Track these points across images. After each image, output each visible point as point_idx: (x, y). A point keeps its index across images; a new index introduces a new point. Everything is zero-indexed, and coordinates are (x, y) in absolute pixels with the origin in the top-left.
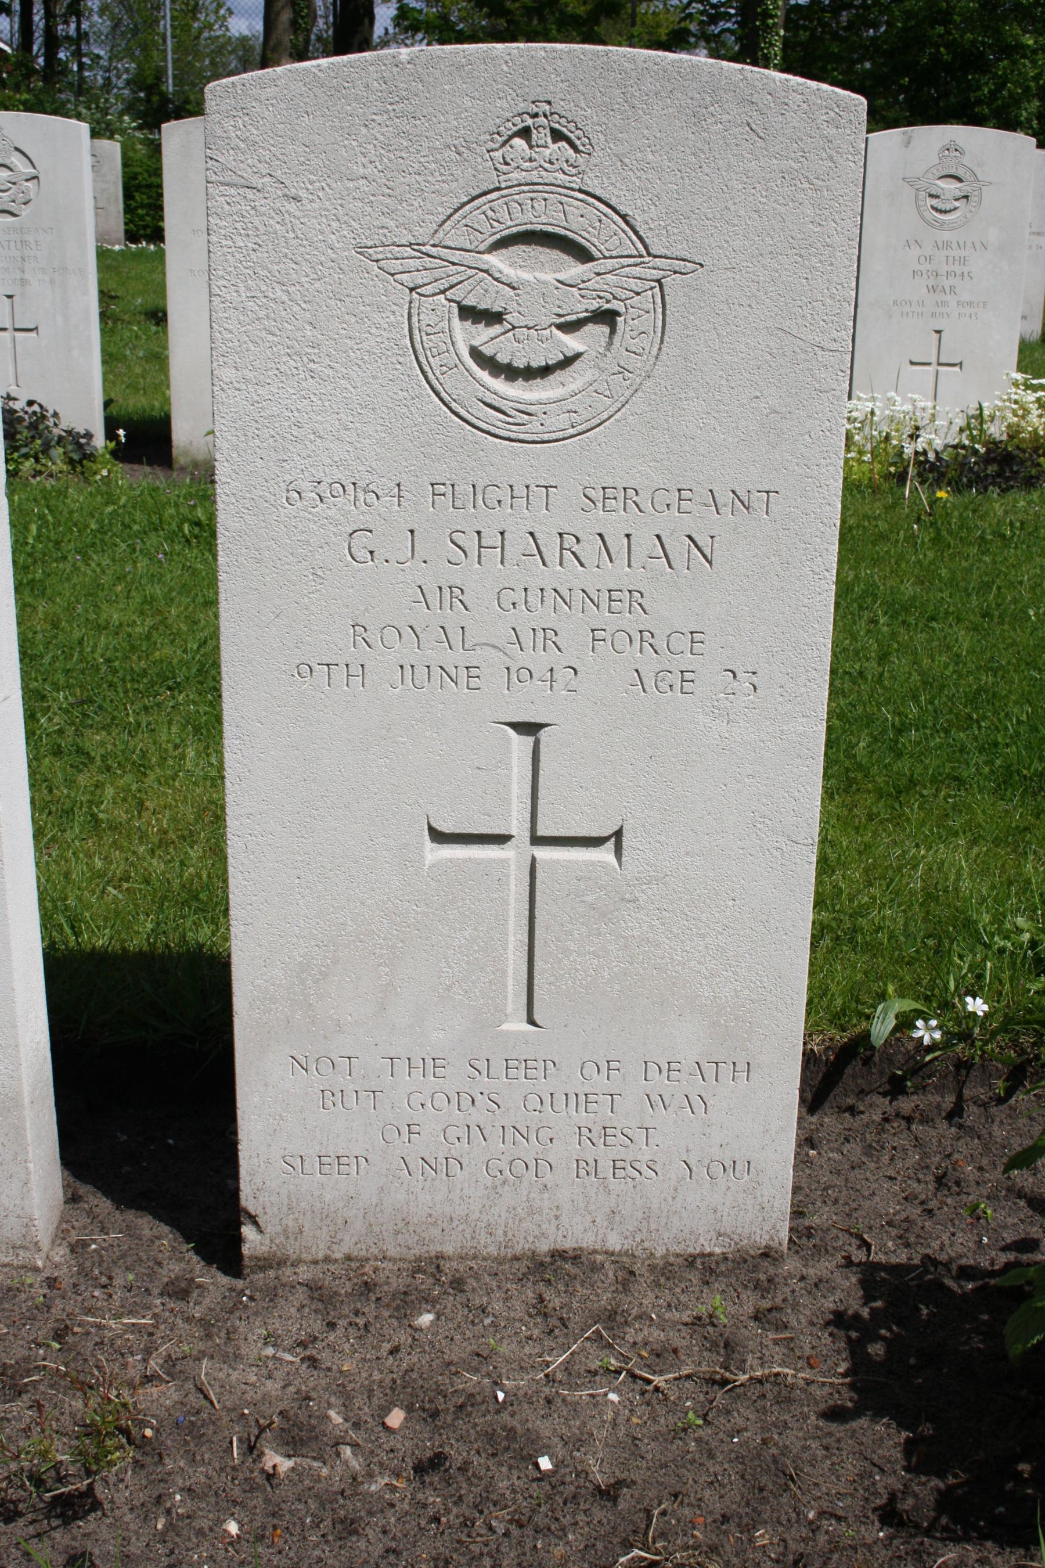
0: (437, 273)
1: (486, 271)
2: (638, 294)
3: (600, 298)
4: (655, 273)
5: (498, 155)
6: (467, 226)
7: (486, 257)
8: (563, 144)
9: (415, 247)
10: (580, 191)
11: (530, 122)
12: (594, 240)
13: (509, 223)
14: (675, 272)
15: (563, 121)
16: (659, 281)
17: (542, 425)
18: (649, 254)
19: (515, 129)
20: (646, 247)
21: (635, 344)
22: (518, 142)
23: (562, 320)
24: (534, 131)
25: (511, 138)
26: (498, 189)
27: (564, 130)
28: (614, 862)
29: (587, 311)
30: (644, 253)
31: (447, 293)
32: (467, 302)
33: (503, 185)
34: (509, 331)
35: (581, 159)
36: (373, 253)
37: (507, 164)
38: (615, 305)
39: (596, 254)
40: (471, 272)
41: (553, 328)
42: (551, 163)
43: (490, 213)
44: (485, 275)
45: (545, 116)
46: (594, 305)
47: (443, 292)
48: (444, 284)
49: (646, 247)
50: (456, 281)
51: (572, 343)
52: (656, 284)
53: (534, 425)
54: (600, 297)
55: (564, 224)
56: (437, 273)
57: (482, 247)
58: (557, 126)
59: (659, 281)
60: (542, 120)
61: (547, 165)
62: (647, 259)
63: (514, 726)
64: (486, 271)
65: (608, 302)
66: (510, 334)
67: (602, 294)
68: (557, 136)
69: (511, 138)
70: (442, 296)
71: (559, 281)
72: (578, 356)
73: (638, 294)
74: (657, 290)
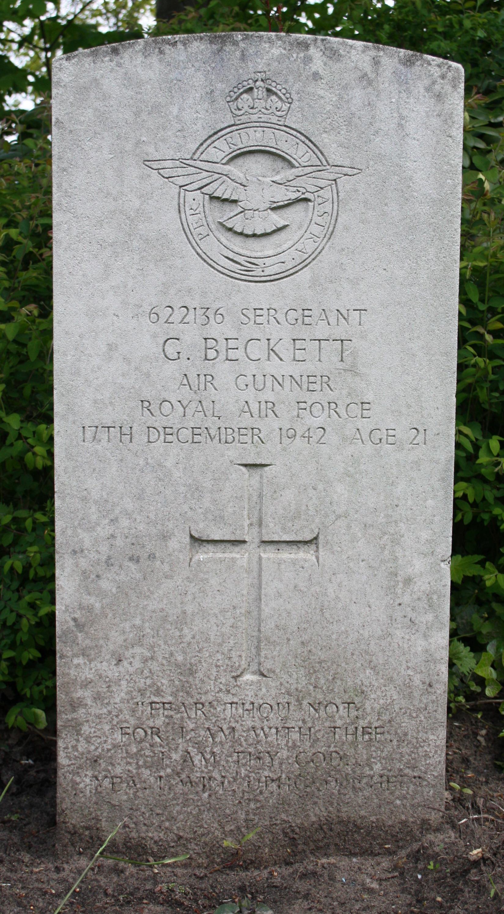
1: (226, 175)
2: (322, 188)
3: (299, 191)
4: (332, 177)
5: (233, 106)
6: (215, 147)
7: (225, 167)
8: (274, 98)
12: (295, 156)
13: (241, 146)
14: (345, 175)
15: (274, 84)
16: (335, 180)
17: (263, 271)
18: (329, 165)
21: (319, 220)
23: (275, 205)
24: (256, 90)
25: (241, 94)
27: (274, 89)
29: (290, 200)
31: (203, 190)
32: (215, 195)
34: (242, 212)
35: (285, 107)
36: (155, 165)
37: (239, 110)
38: (307, 195)
39: (297, 165)
40: (217, 176)
41: (269, 211)
42: (267, 109)
44: (225, 177)
45: (262, 80)
47: (200, 189)
49: (327, 161)
50: (208, 182)
52: (334, 182)
53: (258, 272)
54: (299, 191)
55: (275, 146)
56: (197, 177)
57: (224, 161)
58: (270, 87)
60: (259, 83)
61: (263, 110)
62: (328, 167)
63: (245, 465)
64: (226, 175)
65: (303, 193)
66: (243, 214)
67: (299, 189)
69: (241, 94)
71: (273, 181)
72: (285, 227)
73: (322, 188)
74: (334, 186)
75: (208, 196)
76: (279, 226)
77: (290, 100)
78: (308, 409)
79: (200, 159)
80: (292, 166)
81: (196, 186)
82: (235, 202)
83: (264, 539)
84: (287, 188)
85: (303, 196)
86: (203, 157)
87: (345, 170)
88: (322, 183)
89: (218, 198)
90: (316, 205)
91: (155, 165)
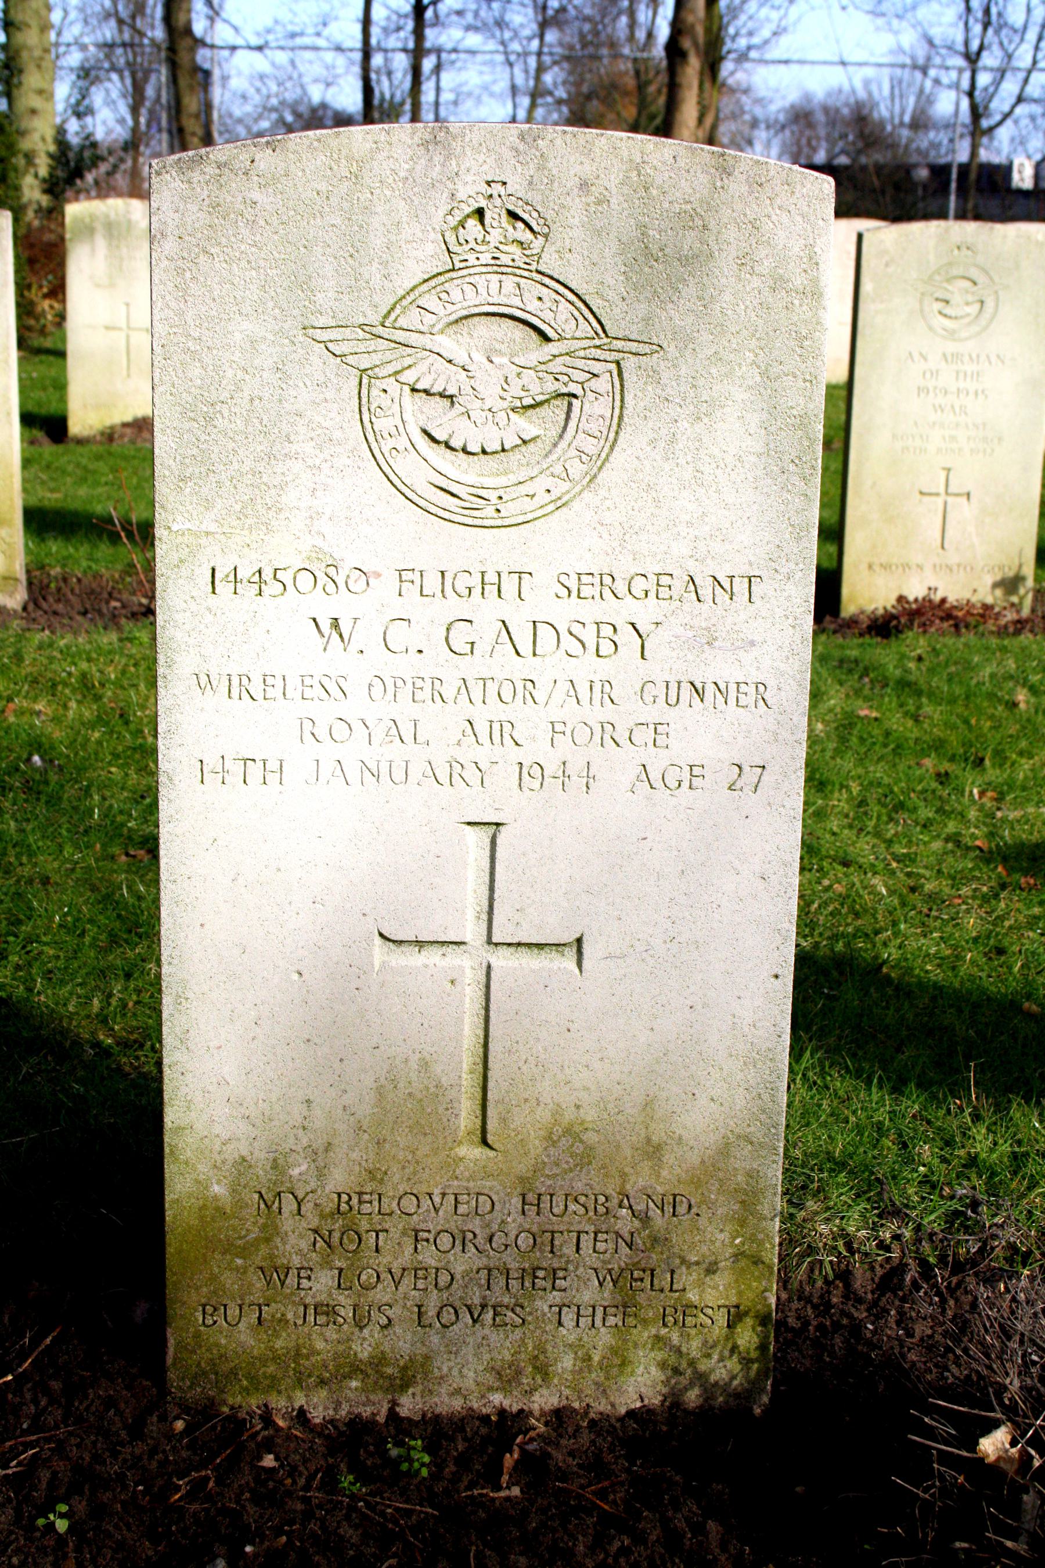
0: (389, 356)
4: (615, 356)
8: (520, 225)
9: (366, 328)
10: (539, 272)
11: (483, 203)
13: (465, 304)
18: (607, 336)
19: (468, 210)
20: (604, 331)
22: (472, 223)
26: (453, 270)
28: (573, 966)
30: (603, 335)
33: (458, 265)
36: (319, 335)
41: (511, 413)
43: (444, 296)
46: (551, 386)
48: (396, 366)
51: (526, 426)
54: (557, 380)
59: (618, 363)
62: (606, 340)
68: (513, 215)
70: (393, 379)
75: (407, 389)
76: (526, 438)
77: (546, 230)
78: (568, 733)
79: (397, 325)
80: (547, 339)
81: (390, 369)
82: (451, 397)
83: (494, 940)
84: (541, 374)
85: (565, 390)
86: (402, 322)
87: (633, 346)
88: (596, 367)
89: (426, 392)
90: (586, 406)
91: (319, 335)
